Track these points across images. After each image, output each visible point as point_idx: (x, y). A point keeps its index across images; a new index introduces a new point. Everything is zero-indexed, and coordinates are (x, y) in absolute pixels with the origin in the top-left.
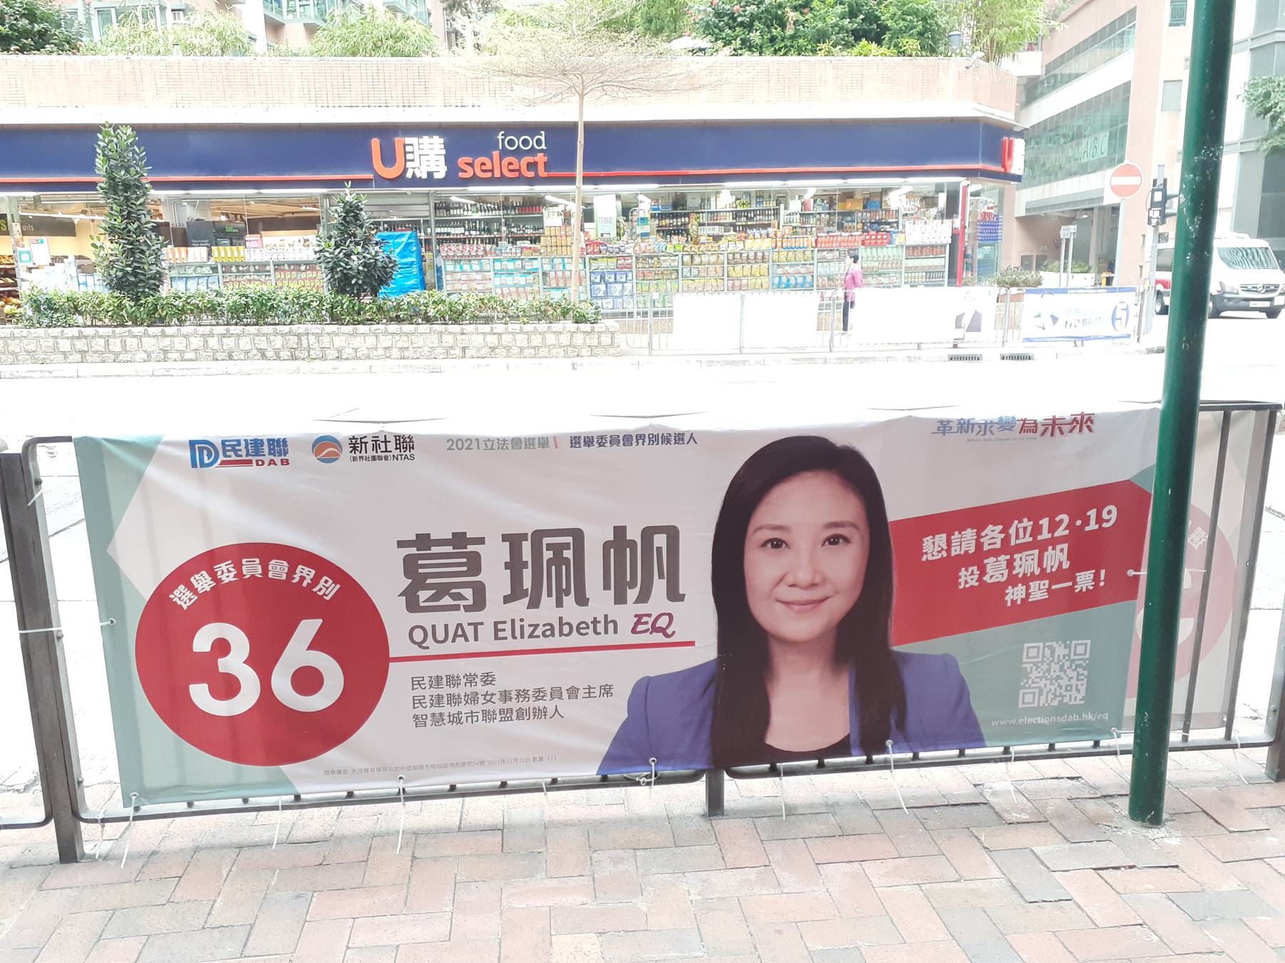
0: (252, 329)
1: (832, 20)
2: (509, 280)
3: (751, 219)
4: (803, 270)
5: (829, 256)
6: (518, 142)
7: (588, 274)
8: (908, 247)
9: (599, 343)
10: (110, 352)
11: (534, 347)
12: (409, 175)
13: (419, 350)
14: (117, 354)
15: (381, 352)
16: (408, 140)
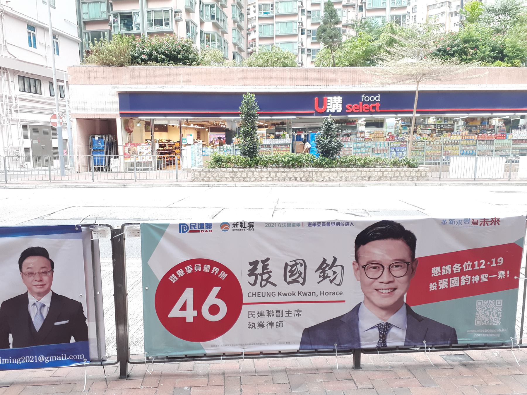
0: (282, 170)
1: (487, 53)
2: (359, 151)
3: (442, 128)
4: (472, 148)
5: (483, 143)
6: (370, 99)
7: (389, 148)
8: (513, 140)
9: (421, 175)
10: (242, 178)
11: (396, 177)
12: (328, 111)
13: (352, 178)
14: (244, 178)
15: (338, 178)
16: (329, 98)
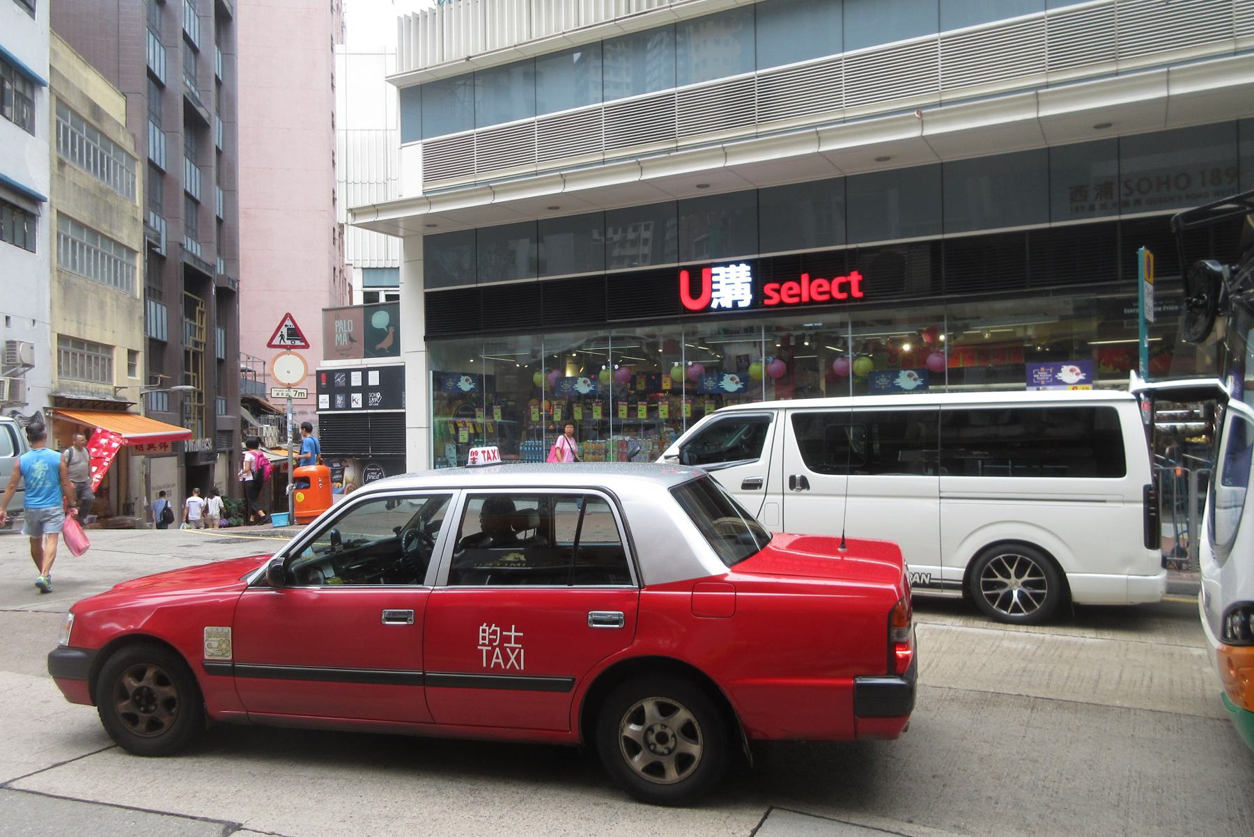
12: (714, 305)
16: (714, 270)
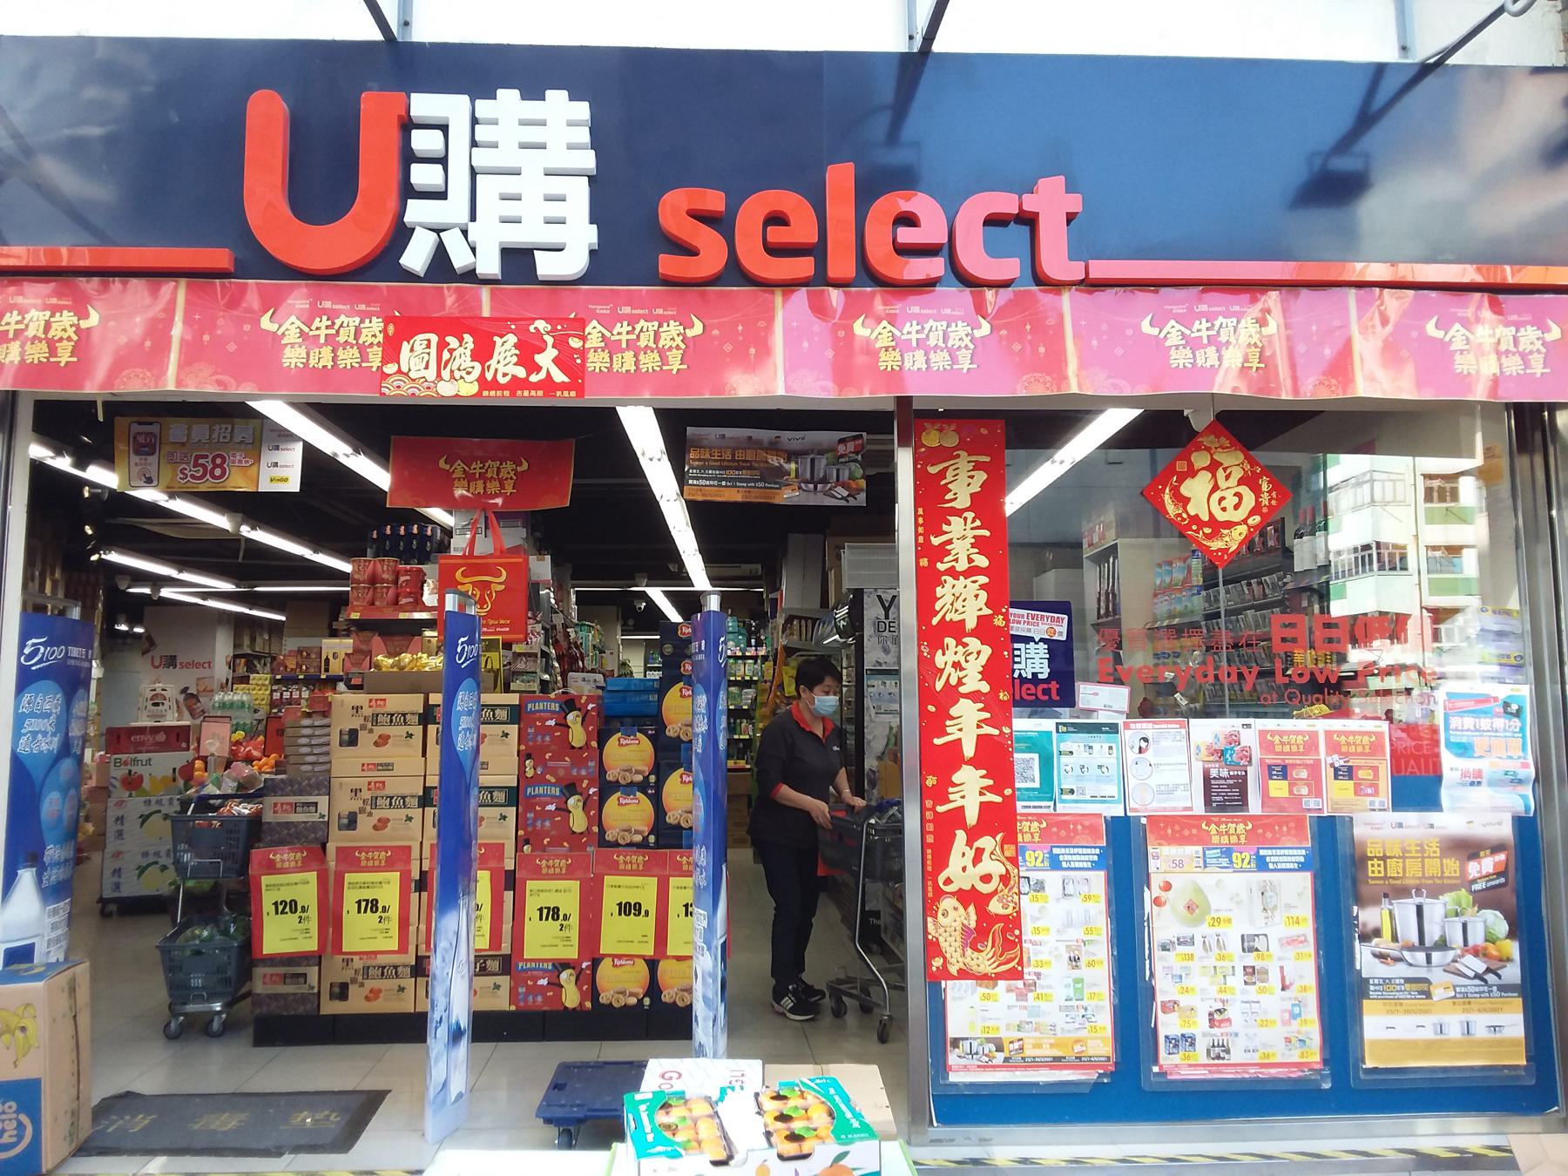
16: (423, 105)
